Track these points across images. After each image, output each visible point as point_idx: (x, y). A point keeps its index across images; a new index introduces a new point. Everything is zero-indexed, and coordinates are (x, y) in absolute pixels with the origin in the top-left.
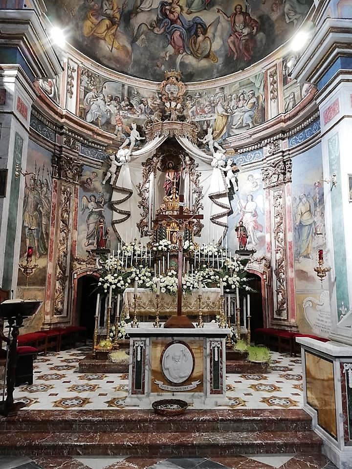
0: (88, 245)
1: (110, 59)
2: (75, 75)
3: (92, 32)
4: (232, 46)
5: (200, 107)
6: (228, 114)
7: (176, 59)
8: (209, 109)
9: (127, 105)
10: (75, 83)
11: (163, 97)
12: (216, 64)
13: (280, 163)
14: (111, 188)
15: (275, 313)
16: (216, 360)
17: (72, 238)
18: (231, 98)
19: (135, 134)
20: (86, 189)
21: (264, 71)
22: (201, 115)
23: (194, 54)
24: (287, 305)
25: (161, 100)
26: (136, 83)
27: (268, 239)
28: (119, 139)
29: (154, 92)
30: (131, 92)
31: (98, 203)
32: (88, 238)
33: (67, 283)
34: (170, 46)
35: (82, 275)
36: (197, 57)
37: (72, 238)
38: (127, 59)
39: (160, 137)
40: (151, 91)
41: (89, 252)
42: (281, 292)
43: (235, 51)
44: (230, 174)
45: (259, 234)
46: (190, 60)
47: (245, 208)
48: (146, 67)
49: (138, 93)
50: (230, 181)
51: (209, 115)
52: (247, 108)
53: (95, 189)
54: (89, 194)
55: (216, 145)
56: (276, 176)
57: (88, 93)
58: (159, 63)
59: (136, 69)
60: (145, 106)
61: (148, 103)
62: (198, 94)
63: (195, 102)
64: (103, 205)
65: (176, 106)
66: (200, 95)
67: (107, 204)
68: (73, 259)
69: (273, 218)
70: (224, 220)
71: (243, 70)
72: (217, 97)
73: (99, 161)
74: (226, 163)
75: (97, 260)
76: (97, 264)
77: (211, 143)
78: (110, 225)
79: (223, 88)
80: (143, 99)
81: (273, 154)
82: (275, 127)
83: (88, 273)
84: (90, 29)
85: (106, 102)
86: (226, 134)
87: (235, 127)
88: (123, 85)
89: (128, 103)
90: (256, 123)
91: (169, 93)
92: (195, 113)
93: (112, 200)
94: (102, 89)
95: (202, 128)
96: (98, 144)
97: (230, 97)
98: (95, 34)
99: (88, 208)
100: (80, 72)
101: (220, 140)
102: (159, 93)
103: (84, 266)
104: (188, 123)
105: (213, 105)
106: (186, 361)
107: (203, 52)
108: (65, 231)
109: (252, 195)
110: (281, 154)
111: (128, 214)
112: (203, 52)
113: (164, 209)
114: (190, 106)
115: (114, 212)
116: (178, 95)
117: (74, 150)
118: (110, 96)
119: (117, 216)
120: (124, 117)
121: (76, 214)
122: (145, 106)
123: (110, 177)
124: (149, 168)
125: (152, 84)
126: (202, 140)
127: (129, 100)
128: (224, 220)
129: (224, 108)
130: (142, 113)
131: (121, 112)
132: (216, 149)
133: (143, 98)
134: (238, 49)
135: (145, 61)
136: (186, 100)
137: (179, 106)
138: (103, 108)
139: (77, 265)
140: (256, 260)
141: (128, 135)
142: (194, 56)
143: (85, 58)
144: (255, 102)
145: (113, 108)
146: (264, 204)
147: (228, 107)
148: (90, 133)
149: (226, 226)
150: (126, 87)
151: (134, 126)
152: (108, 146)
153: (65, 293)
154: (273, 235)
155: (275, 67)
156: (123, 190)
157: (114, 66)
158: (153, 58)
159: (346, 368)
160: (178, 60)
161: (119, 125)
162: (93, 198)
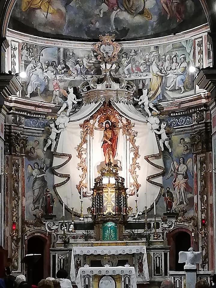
0: (34, 210)
1: (45, 25)
2: (16, 53)
3: (29, 5)
4: (164, 6)
5: (136, 66)
6: (163, 75)
7: (110, 16)
8: (145, 68)
9: (63, 68)
10: (17, 60)
11: (99, 57)
12: (150, 21)
13: (203, 134)
14: (51, 154)
15: (200, 266)
16: (127, 284)
17: (22, 205)
18: (165, 58)
19: (72, 98)
20: (30, 158)
21: (193, 38)
22: (137, 73)
23: (128, 10)
24: (208, 259)
25: (97, 59)
26: (71, 46)
27: (195, 201)
28: (57, 104)
29: (90, 51)
30: (67, 55)
31: (41, 169)
32: (34, 203)
33: (20, 244)
34: (104, 4)
35: (30, 237)
36: (131, 13)
37: (22, 205)
38: (61, 21)
39: (96, 103)
40: (86, 50)
41: (35, 215)
42: (205, 248)
43: (168, 11)
44: (164, 137)
45: (190, 195)
46: (124, 16)
47: (178, 170)
48: (81, 26)
49: (73, 53)
50: (164, 144)
51: (145, 74)
52: (179, 71)
53: (38, 157)
54: (33, 162)
55: (151, 106)
56: (200, 143)
57: (27, 65)
58: (93, 21)
59: (71, 30)
60: (81, 66)
61: (83, 63)
62: (133, 51)
63: (131, 60)
64: (45, 171)
65: (112, 66)
66: (135, 52)
67: (48, 169)
68: (24, 223)
69: (199, 182)
70: (159, 180)
71: (175, 34)
72: (152, 55)
73: (40, 130)
74: (160, 123)
75: (46, 225)
76: (46, 227)
77: (146, 104)
78: (52, 188)
79: (157, 47)
80: (78, 60)
81: (199, 124)
82: (198, 102)
83: (36, 234)
84: (27, 3)
85: (43, 70)
86: (161, 95)
87: (169, 89)
88: (59, 49)
89: (64, 66)
90: (187, 89)
91: (104, 52)
92: (131, 71)
93: (54, 165)
94: (40, 58)
95: (138, 87)
96: (38, 114)
97: (164, 57)
98: (32, 6)
99: (33, 175)
100: (20, 49)
101: (155, 101)
102: (94, 52)
103: (32, 229)
104: (123, 88)
105: (148, 64)
106: (111, 285)
107: (137, 9)
108: (16, 199)
109: (183, 158)
110: (204, 124)
111: (68, 177)
112: (137, 9)
113: (100, 180)
114: (126, 64)
115: (55, 175)
116: (113, 54)
117: (20, 126)
118: (47, 62)
119: (58, 180)
120: (61, 81)
121: (24, 182)
122: (81, 66)
123: (51, 144)
124: (87, 129)
125: (87, 44)
126: (138, 100)
127: (64, 61)
128: (159, 180)
129: (158, 68)
130: (78, 74)
131: (58, 76)
132: (151, 110)
133: (79, 58)
134: (170, 10)
135: (79, 19)
136: (121, 57)
137: (114, 66)
138: (41, 77)
139: (27, 227)
140: (186, 220)
141: (65, 99)
142: (128, 12)
143: (24, 36)
144: (186, 67)
145: (50, 75)
146: (193, 168)
147: (162, 67)
148: (33, 108)
149: (161, 186)
150: (62, 50)
151: (71, 90)
152: (47, 115)
153: (19, 252)
154: (199, 197)
155: (201, 39)
156: (63, 155)
157: (47, 31)
158: (87, 16)
159: (176, 280)
160: (113, 16)
161: (57, 90)
162: (36, 166)
